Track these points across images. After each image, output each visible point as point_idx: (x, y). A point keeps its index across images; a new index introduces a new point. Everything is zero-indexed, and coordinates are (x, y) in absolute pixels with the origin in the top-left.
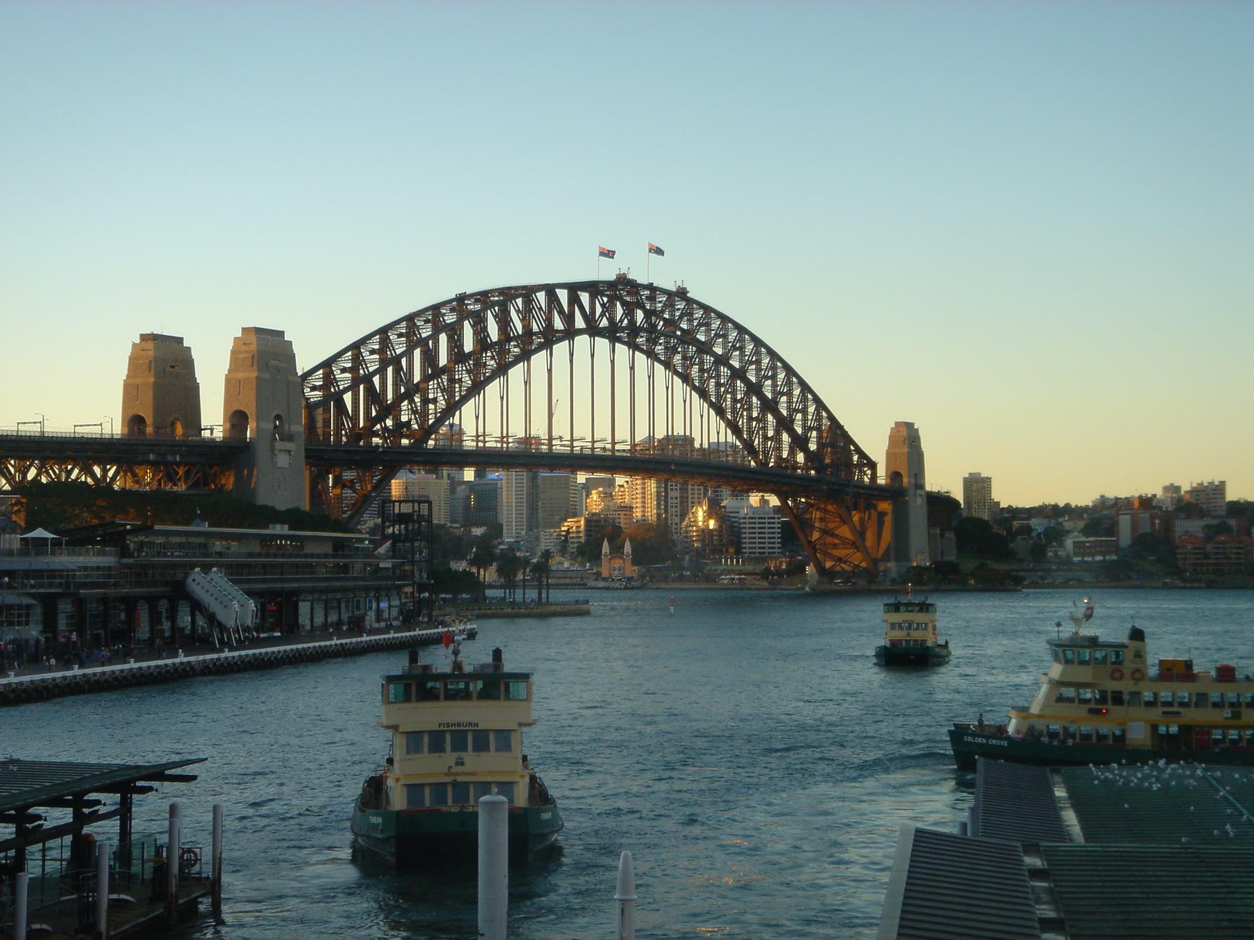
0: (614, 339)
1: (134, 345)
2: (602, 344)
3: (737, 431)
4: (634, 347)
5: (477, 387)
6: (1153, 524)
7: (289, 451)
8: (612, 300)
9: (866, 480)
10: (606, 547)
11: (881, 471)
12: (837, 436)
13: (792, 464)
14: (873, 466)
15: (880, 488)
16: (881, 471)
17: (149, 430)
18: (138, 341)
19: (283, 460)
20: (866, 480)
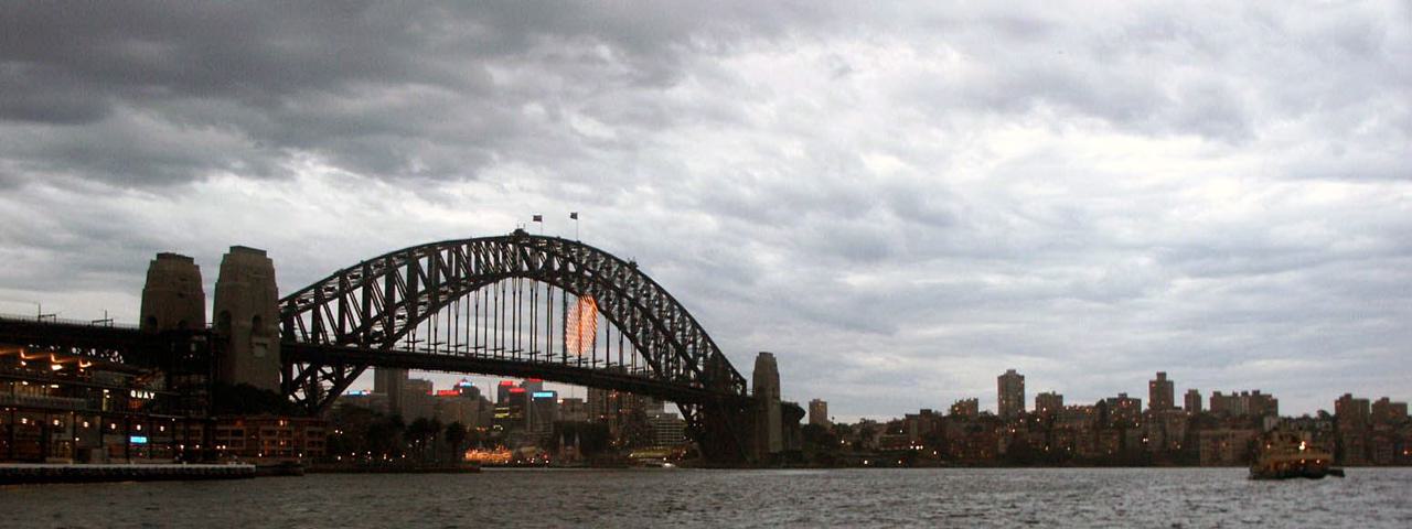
0: (552, 283)
1: (152, 262)
2: (543, 285)
3: (646, 354)
4: (567, 289)
5: (434, 308)
6: (932, 426)
7: (265, 345)
8: (552, 254)
9: (739, 391)
10: (562, 441)
11: (750, 385)
12: (719, 363)
13: (685, 378)
14: (744, 382)
15: (749, 398)
16: (750, 385)
17: (160, 327)
18: (155, 258)
19: (260, 352)
20: (739, 391)
